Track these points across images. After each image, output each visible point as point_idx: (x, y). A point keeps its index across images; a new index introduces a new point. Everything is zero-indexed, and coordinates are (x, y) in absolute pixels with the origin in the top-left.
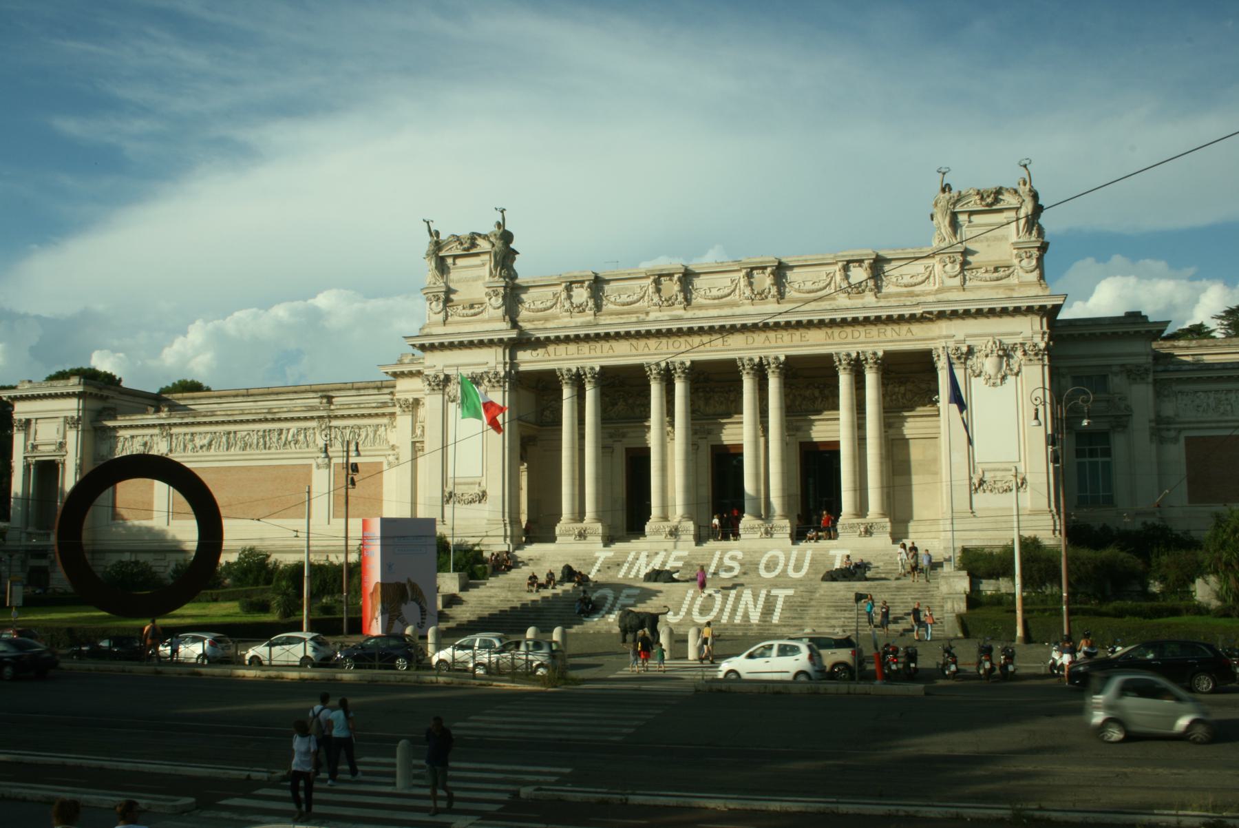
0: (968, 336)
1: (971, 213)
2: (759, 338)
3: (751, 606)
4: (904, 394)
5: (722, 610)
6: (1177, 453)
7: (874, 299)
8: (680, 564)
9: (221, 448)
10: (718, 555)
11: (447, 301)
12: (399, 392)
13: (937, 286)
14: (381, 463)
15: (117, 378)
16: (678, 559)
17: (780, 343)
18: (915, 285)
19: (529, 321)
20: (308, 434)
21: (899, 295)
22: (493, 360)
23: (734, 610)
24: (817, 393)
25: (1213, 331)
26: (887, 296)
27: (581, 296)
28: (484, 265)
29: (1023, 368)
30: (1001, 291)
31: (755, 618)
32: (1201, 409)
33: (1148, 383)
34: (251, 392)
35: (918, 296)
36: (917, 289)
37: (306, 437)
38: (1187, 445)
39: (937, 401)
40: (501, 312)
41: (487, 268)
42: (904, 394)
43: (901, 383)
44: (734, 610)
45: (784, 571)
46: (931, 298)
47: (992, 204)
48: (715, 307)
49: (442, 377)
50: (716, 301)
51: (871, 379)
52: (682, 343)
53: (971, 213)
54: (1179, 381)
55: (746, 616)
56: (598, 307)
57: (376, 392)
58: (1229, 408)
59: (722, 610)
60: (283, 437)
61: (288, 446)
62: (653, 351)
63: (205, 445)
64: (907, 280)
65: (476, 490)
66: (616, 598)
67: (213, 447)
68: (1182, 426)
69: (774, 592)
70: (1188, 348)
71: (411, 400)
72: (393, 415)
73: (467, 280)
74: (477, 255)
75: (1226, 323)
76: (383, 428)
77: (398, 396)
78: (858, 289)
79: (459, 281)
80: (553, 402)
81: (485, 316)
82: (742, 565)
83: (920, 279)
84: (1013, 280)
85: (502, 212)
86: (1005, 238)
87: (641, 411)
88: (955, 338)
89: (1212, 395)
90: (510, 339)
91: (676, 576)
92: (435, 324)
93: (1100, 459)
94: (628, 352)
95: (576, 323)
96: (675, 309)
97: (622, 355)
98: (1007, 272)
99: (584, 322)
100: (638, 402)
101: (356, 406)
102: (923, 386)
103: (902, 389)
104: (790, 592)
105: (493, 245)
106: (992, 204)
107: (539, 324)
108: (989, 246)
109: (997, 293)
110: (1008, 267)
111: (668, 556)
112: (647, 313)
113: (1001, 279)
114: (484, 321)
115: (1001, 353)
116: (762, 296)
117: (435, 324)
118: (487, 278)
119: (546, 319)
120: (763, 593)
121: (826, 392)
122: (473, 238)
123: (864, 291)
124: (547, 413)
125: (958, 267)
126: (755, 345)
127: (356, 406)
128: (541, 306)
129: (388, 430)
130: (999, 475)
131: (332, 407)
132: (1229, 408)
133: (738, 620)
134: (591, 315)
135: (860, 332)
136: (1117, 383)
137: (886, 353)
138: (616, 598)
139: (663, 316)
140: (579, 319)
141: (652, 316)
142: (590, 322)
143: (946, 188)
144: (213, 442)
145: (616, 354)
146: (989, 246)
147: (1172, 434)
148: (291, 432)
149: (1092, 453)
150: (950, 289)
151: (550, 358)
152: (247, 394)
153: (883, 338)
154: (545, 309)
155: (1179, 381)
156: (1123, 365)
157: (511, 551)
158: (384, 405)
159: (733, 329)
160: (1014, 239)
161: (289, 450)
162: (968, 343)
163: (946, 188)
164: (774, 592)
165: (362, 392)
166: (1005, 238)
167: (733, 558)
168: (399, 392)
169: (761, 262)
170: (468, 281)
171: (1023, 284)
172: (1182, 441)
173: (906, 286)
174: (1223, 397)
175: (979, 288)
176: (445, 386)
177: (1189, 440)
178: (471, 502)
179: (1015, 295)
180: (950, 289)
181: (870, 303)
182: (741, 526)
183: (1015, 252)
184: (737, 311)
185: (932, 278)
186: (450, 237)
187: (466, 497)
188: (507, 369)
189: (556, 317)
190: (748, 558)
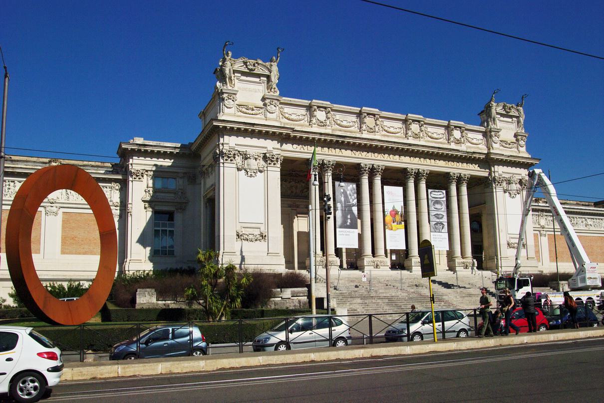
2: (417, 160)
48: (395, 137)
74: (259, 76)
79: (245, 89)
92: (229, 115)
117: (229, 115)
134: (329, 129)
151: (304, 151)
162: (503, 176)
187: (251, 237)
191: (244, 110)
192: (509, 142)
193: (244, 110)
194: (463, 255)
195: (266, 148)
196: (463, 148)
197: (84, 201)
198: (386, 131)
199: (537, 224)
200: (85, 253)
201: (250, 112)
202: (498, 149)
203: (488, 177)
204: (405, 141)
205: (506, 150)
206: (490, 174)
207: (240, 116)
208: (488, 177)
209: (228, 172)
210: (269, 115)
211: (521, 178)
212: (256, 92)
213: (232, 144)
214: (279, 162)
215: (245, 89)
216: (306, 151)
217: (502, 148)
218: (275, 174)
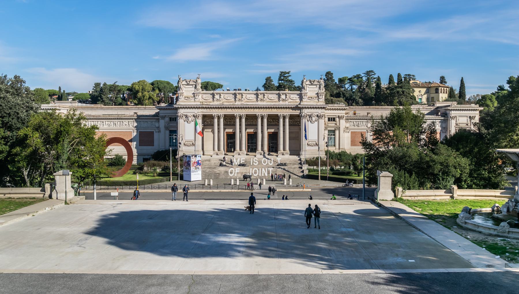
2: (262, 110)
3: (265, 172)
5: (259, 173)
8: (244, 162)
10: (252, 159)
14: (154, 132)
16: (243, 160)
17: (266, 111)
21: (293, 102)
23: (262, 173)
24: (272, 121)
25: (363, 77)
26: (290, 102)
31: (266, 175)
38: (351, 133)
43: (291, 119)
44: (262, 173)
45: (268, 163)
52: (243, 110)
55: (264, 174)
57: (144, 109)
59: (259, 173)
62: (236, 111)
66: (235, 170)
69: (269, 169)
70: (353, 108)
79: (187, 91)
82: (258, 162)
91: (247, 165)
93: (333, 136)
94: (230, 111)
102: (296, 120)
104: (272, 169)
111: (240, 159)
120: (267, 169)
124: (206, 122)
126: (261, 111)
130: (313, 143)
133: (263, 175)
135: (285, 110)
136: (337, 119)
138: (235, 170)
145: (227, 111)
147: (348, 131)
149: (331, 135)
159: (256, 108)
164: (269, 169)
165: (140, 109)
167: (256, 160)
172: (350, 132)
175: (310, 102)
177: (352, 132)
187: (189, 145)
190: (259, 160)
191: (187, 99)
193: (187, 99)
194: (284, 149)
196: (287, 103)
197: (134, 136)
199: (366, 126)
202: (306, 102)
203: (299, 115)
204: (257, 103)
205: (310, 102)
206: (300, 113)
207: (184, 102)
208: (299, 115)
209: (181, 122)
210: (195, 99)
213: (182, 112)
214: (200, 117)
216: (212, 111)
217: (309, 100)
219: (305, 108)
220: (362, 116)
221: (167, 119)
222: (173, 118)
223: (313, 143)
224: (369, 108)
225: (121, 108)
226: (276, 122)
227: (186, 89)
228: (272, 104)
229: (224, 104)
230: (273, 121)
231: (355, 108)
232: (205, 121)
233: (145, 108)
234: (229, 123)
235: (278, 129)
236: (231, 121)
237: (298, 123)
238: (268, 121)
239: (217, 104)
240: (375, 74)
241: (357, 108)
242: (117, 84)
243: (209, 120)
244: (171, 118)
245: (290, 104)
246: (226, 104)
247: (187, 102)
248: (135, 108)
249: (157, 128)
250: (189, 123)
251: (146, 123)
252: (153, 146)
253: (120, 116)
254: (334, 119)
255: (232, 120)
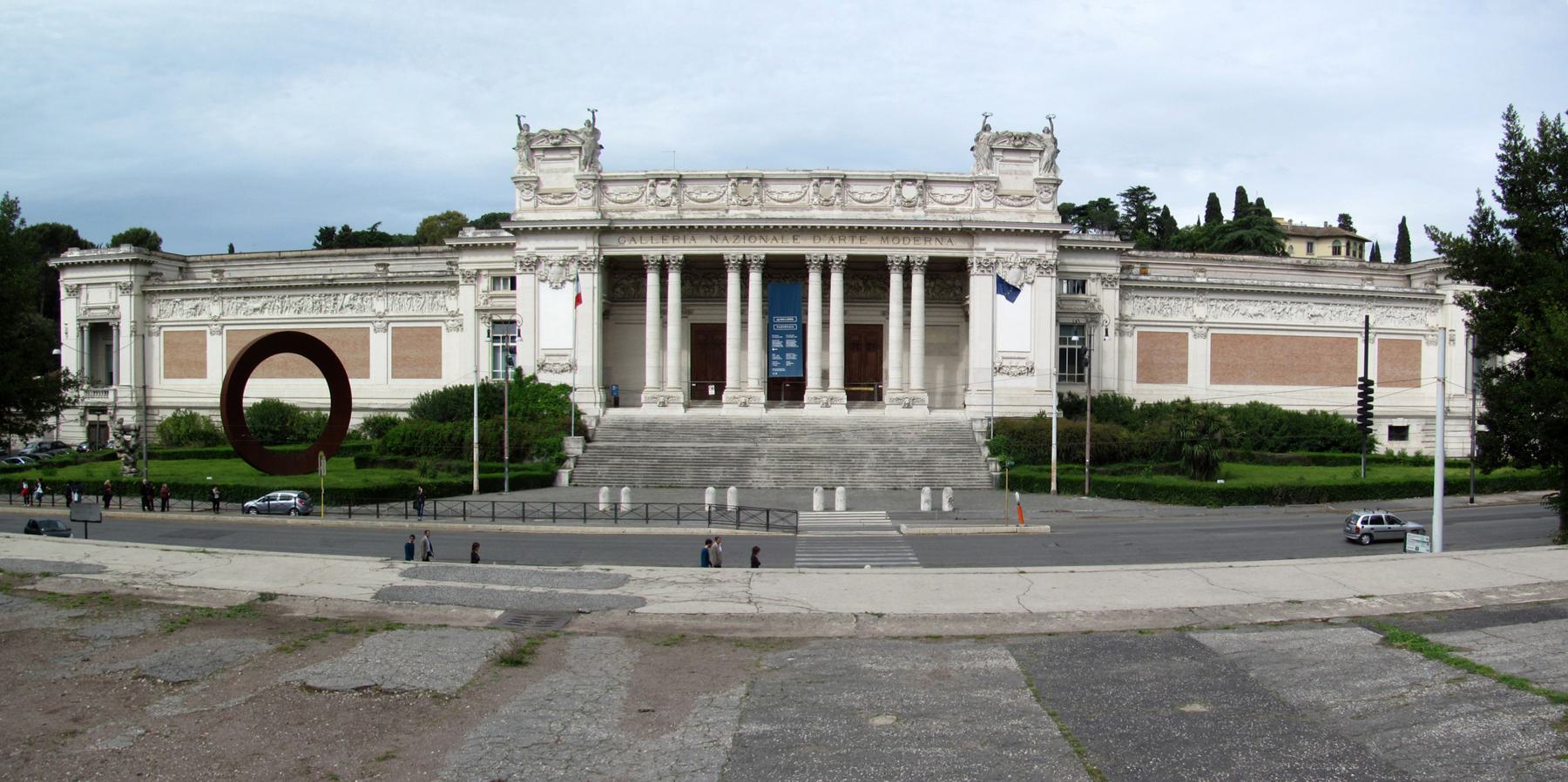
0: (996, 250)
1: (1005, 150)
2: (825, 242)
4: (934, 288)
6: (1131, 343)
7: (922, 213)
9: (275, 311)
11: (537, 189)
12: (461, 263)
13: (973, 207)
15: (152, 233)
18: (957, 203)
19: (616, 211)
20: (365, 299)
21: (943, 211)
22: (585, 246)
25: (1117, 206)
26: (933, 212)
27: (667, 191)
28: (575, 158)
29: (1038, 280)
30: (1025, 215)
32: (1150, 311)
33: (1116, 289)
34: (283, 254)
35: (958, 213)
36: (958, 208)
37: (362, 301)
38: (1138, 338)
39: (968, 299)
40: (590, 202)
41: (577, 161)
42: (934, 288)
46: (967, 217)
47: (1022, 146)
48: (787, 209)
49: (535, 259)
50: (788, 204)
51: (918, 280)
53: (1005, 150)
54: (1137, 288)
56: (680, 202)
58: (1169, 311)
60: (340, 303)
61: (342, 311)
63: (258, 309)
64: (949, 199)
65: (565, 361)
67: (266, 311)
68: (1136, 323)
71: (475, 272)
72: (455, 284)
73: (557, 171)
74: (568, 149)
75: (1128, 200)
76: (441, 295)
77: (461, 267)
78: (910, 205)
79: (549, 171)
80: (625, 281)
81: (574, 205)
83: (960, 199)
84: (1033, 209)
85: (593, 113)
86: (1029, 173)
87: (705, 292)
88: (987, 251)
89: (1158, 300)
90: (601, 227)
95: (662, 216)
96: (752, 209)
97: (703, 247)
98: (1029, 202)
99: (667, 216)
100: (703, 283)
101: (414, 274)
102: (949, 282)
103: (932, 283)
105: (583, 143)
106: (1022, 146)
107: (627, 215)
108: (1017, 178)
109: (1022, 218)
110: (1031, 197)
112: (727, 211)
113: (1022, 206)
114: (574, 210)
115: (1021, 265)
116: (827, 203)
118: (577, 172)
119: (633, 211)
121: (869, 283)
122: (565, 134)
123: (914, 206)
124: (618, 290)
125: (992, 193)
127: (414, 274)
128: (627, 198)
129: (447, 298)
130: (1014, 362)
131: (389, 275)
132: (1169, 311)
136: (1093, 287)
137: (931, 258)
139: (741, 214)
140: (663, 213)
141: (732, 213)
142: (674, 215)
143: (986, 128)
144: (267, 306)
146: (1017, 178)
147: (1129, 328)
148: (348, 297)
150: (985, 211)
152: (280, 257)
153: (928, 245)
154: (632, 201)
155: (1137, 288)
156: (1099, 274)
157: (601, 415)
158: (442, 274)
160: (1036, 175)
161: (346, 315)
162: (996, 255)
163: (986, 128)
166: (1029, 173)
168: (461, 263)
169: (830, 174)
170: (558, 172)
171: (1040, 212)
173: (948, 204)
174: (1166, 302)
176: (536, 267)
178: (562, 371)
179: (1035, 221)
180: (985, 211)
181: (919, 216)
182: (805, 396)
183: (1036, 187)
184: (807, 214)
185: (969, 199)
186: (540, 132)
187: (557, 367)
188: (597, 253)
189: (643, 210)
192: (1016, 196)
193: (549, 200)
195: (577, 248)
196: (919, 213)
198: (775, 200)
200: (418, 377)
201: (559, 201)
211: (1036, 257)
212: (565, 172)
215: (549, 171)
218: (591, 283)
219: (988, 233)
220: (1177, 279)
221: (485, 283)
222: (505, 279)
223: (1014, 362)
224: (1192, 258)
225: (341, 255)
226: (878, 291)
227: (544, 166)
228: (866, 215)
229: (686, 216)
230: (864, 283)
231: (1147, 257)
232: (616, 286)
233: (418, 253)
234: (702, 291)
235: (886, 314)
236: (710, 283)
237: (958, 292)
238: (848, 287)
239: (659, 217)
240: (1154, 198)
241: (1153, 258)
242: (380, 229)
243: (632, 281)
244: (496, 280)
245: (930, 217)
246: (691, 216)
247: (549, 210)
248: (386, 254)
249: (453, 316)
250: (557, 288)
251: (415, 297)
252: (440, 377)
253: (330, 277)
254: (1080, 286)
255: (715, 281)
